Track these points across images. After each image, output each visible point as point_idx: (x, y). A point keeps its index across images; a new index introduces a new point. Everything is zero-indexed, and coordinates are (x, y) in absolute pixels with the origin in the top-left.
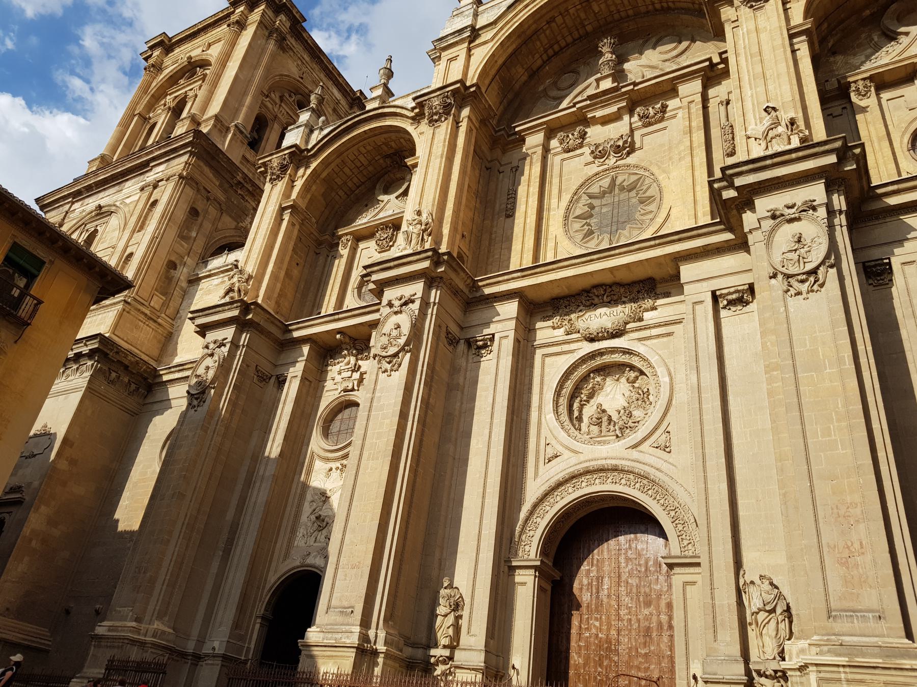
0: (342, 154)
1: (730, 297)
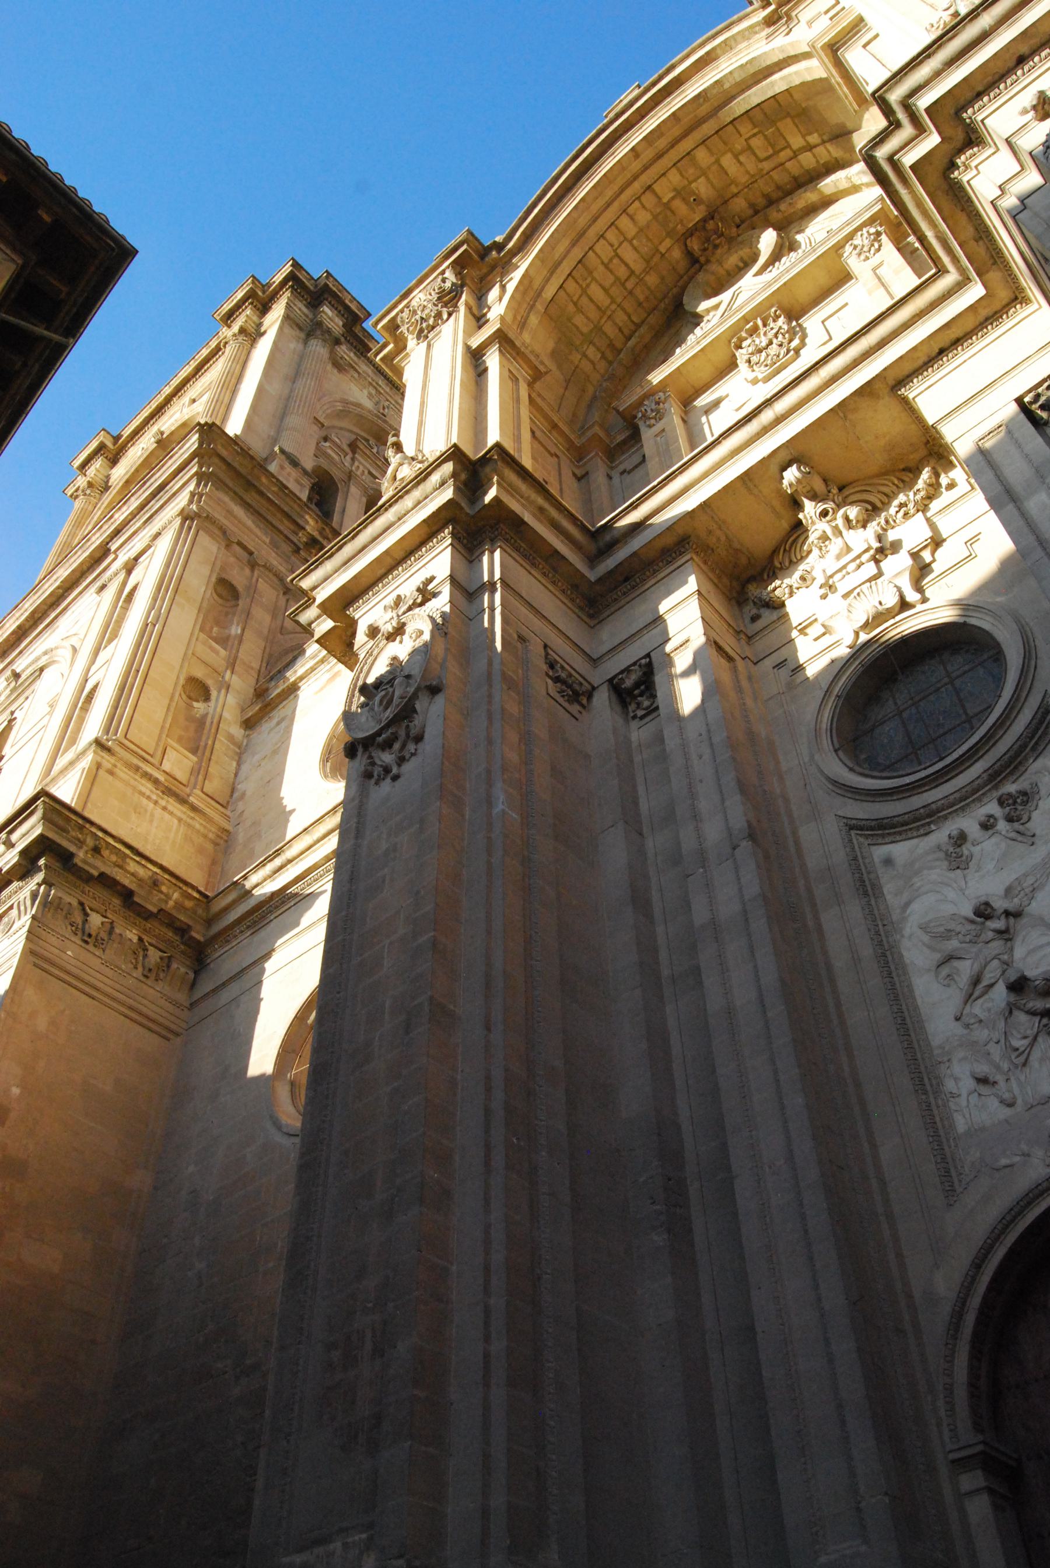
0: (582, 234)
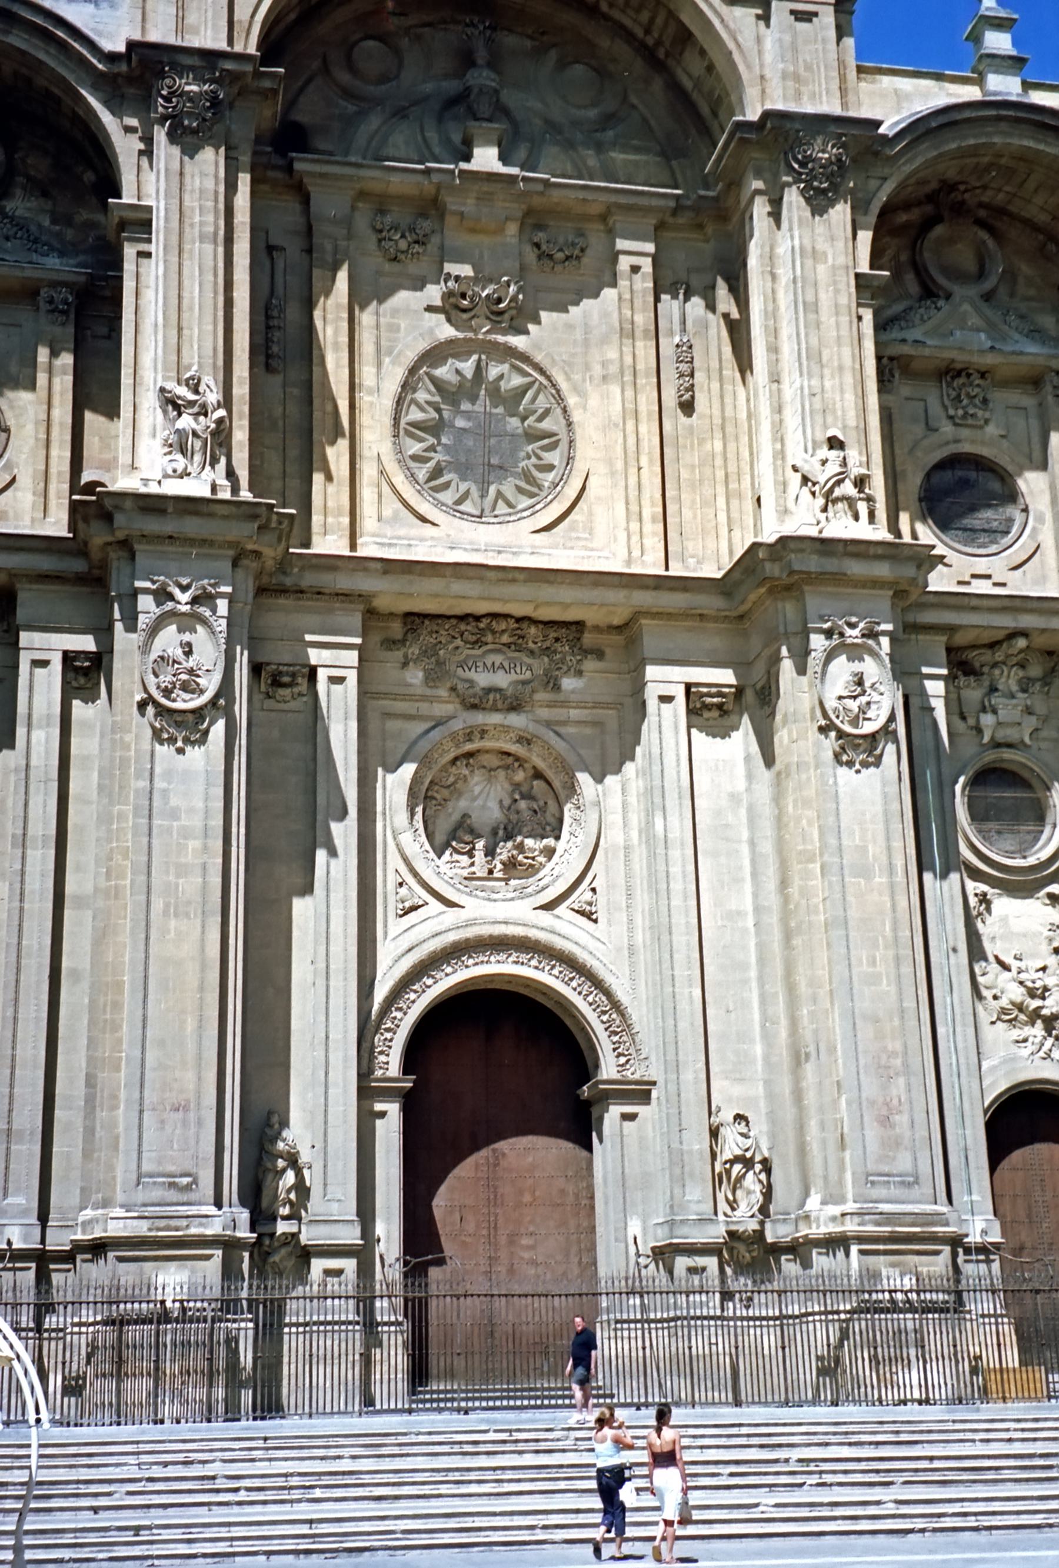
1: (709, 700)
